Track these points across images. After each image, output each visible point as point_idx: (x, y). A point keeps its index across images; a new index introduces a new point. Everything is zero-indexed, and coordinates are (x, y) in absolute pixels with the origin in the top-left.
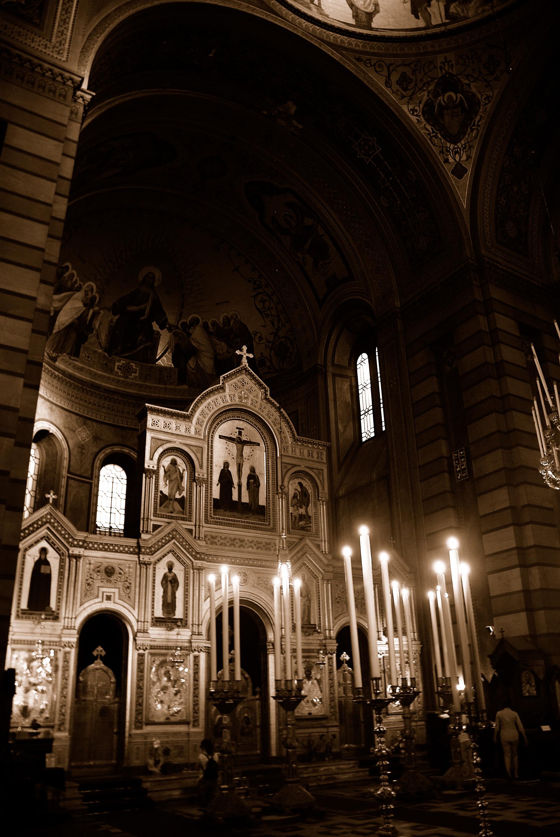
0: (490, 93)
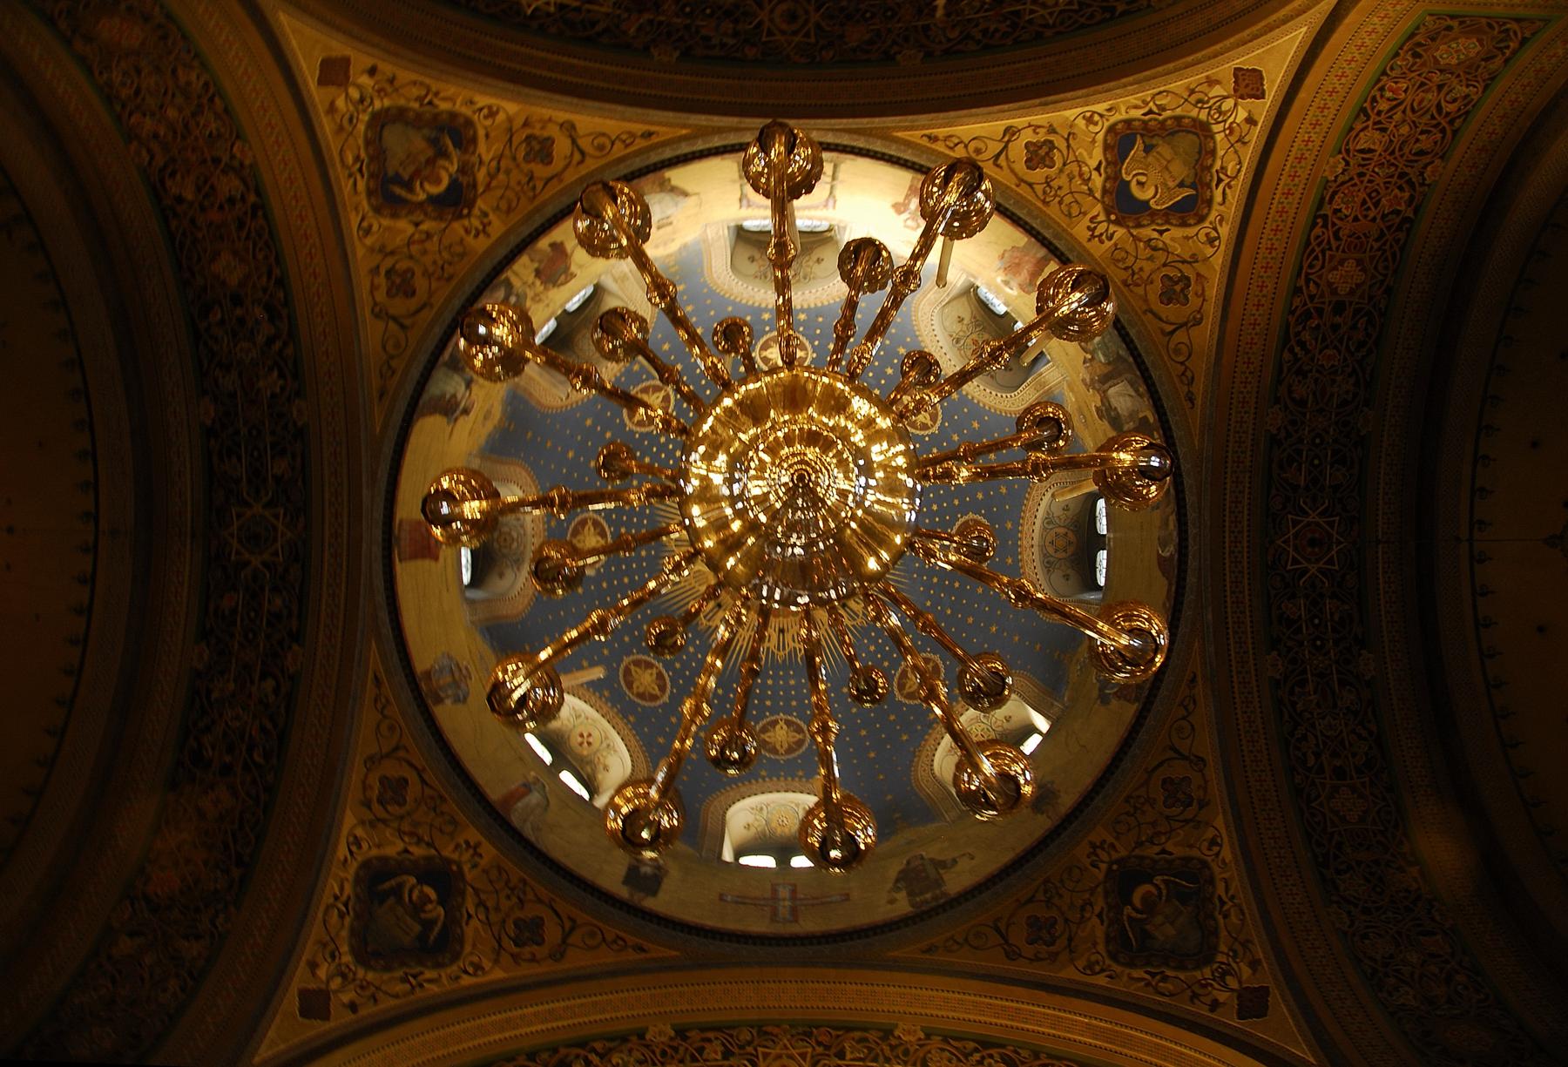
0: (369, 241)
